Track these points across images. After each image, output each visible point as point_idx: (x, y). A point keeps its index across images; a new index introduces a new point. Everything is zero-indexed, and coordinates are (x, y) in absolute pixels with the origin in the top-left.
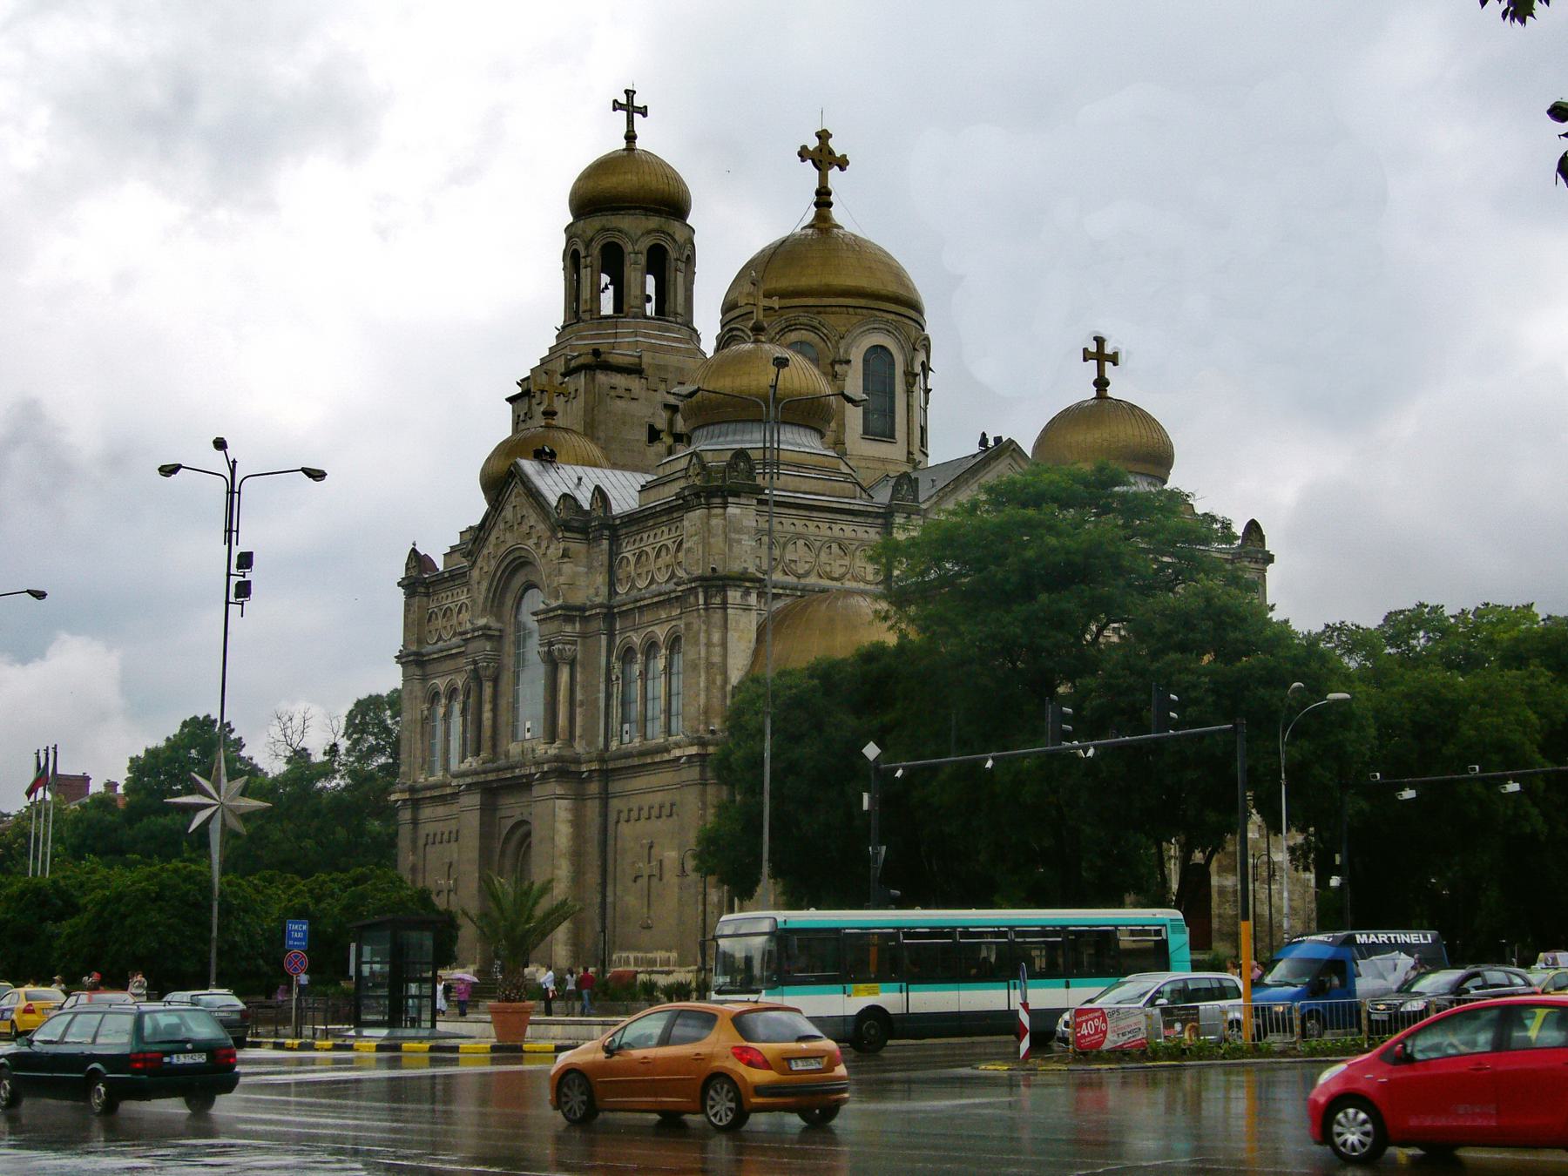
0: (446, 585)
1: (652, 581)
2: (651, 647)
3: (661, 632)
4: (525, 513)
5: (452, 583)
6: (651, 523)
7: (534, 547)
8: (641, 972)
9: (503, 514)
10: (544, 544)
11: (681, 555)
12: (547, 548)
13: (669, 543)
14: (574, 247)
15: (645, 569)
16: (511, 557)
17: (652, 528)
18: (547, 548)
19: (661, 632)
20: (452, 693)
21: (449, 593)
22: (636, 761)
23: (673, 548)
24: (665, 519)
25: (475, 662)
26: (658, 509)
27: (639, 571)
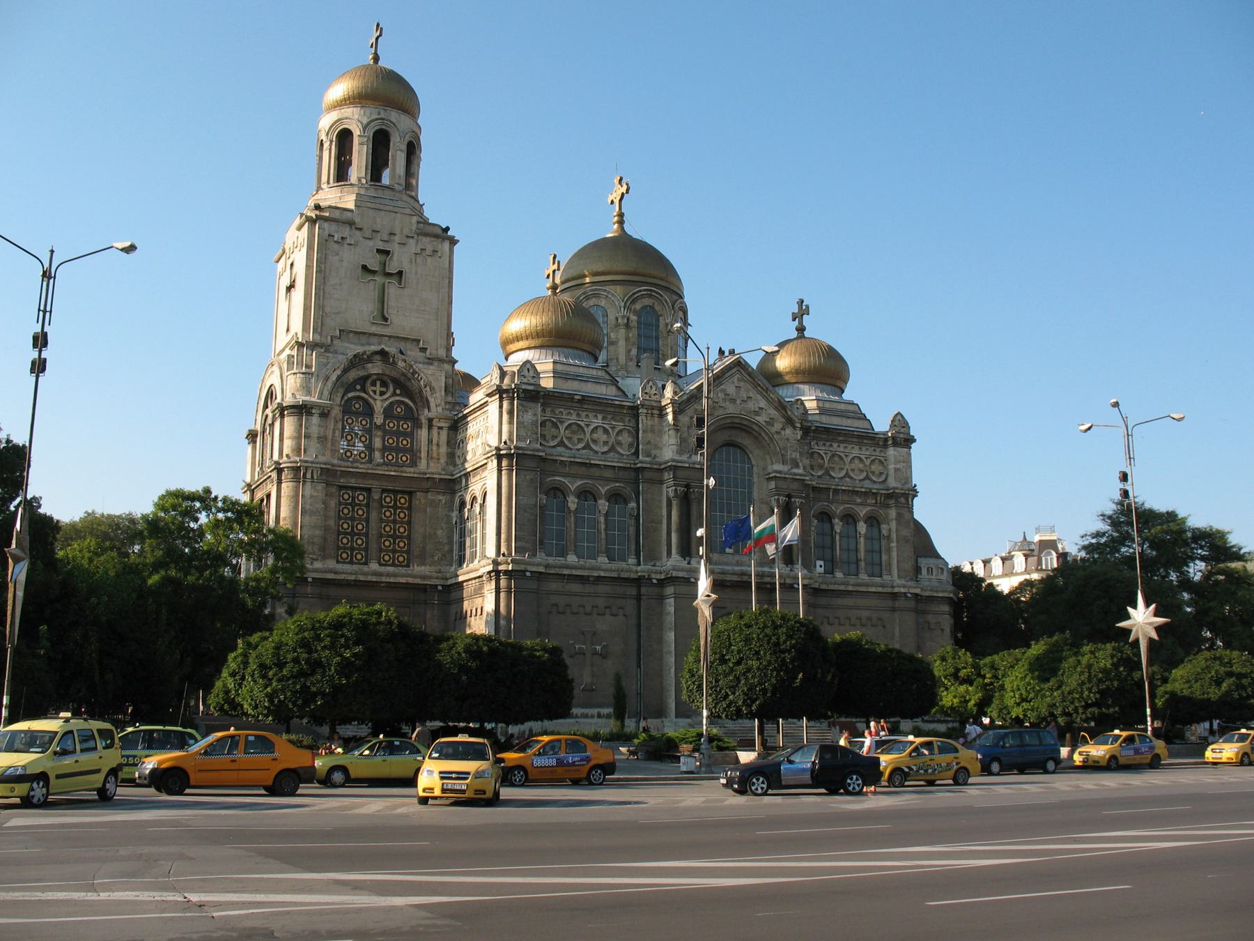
0: (569, 404)
1: (847, 475)
2: (850, 519)
3: (863, 512)
4: (751, 395)
5: (578, 405)
6: (841, 438)
7: (764, 423)
8: (857, 722)
9: (721, 387)
10: (777, 426)
11: (873, 467)
12: (783, 429)
13: (863, 457)
14: (388, 129)
15: (838, 466)
16: (729, 421)
17: (841, 442)
18: (783, 429)
19: (863, 512)
20: (586, 494)
21: (572, 411)
22: (850, 588)
23: (868, 462)
24: (855, 440)
25: (688, 486)
26: (855, 433)
27: (833, 466)
